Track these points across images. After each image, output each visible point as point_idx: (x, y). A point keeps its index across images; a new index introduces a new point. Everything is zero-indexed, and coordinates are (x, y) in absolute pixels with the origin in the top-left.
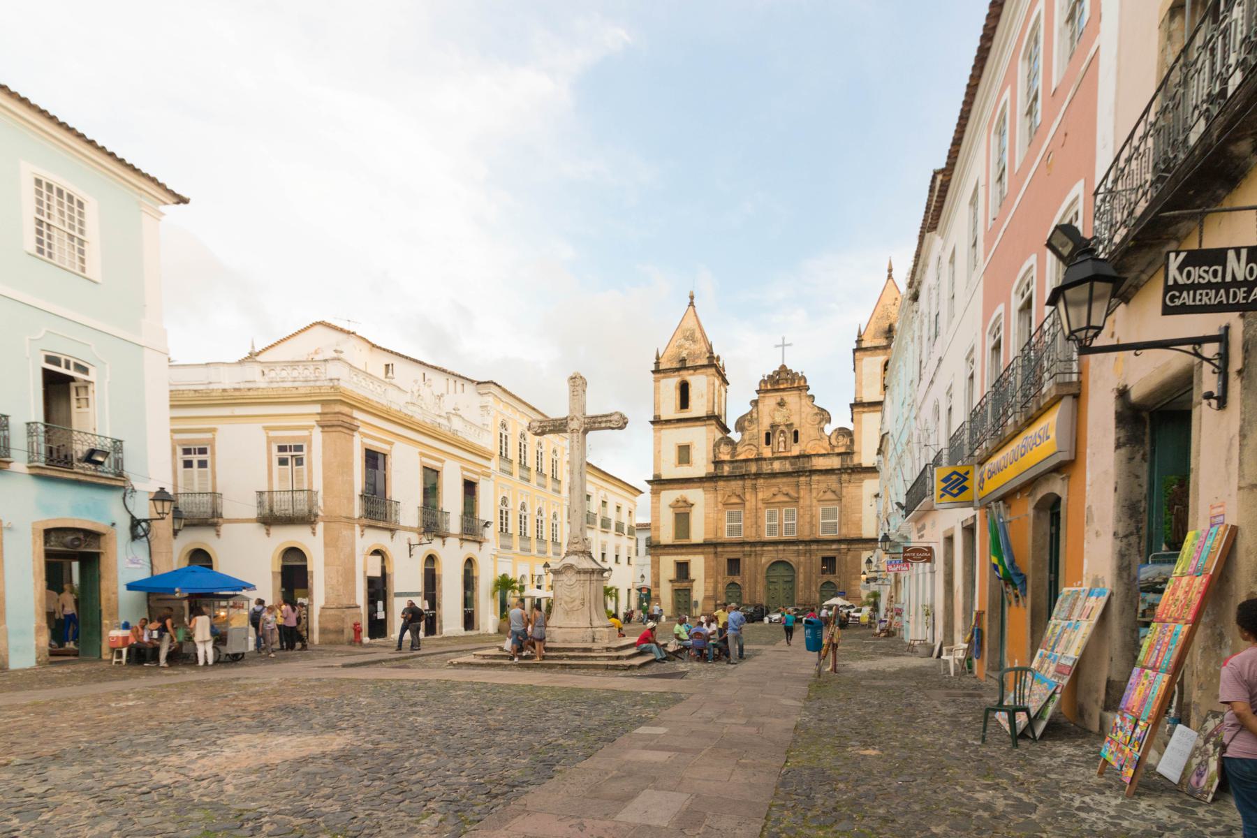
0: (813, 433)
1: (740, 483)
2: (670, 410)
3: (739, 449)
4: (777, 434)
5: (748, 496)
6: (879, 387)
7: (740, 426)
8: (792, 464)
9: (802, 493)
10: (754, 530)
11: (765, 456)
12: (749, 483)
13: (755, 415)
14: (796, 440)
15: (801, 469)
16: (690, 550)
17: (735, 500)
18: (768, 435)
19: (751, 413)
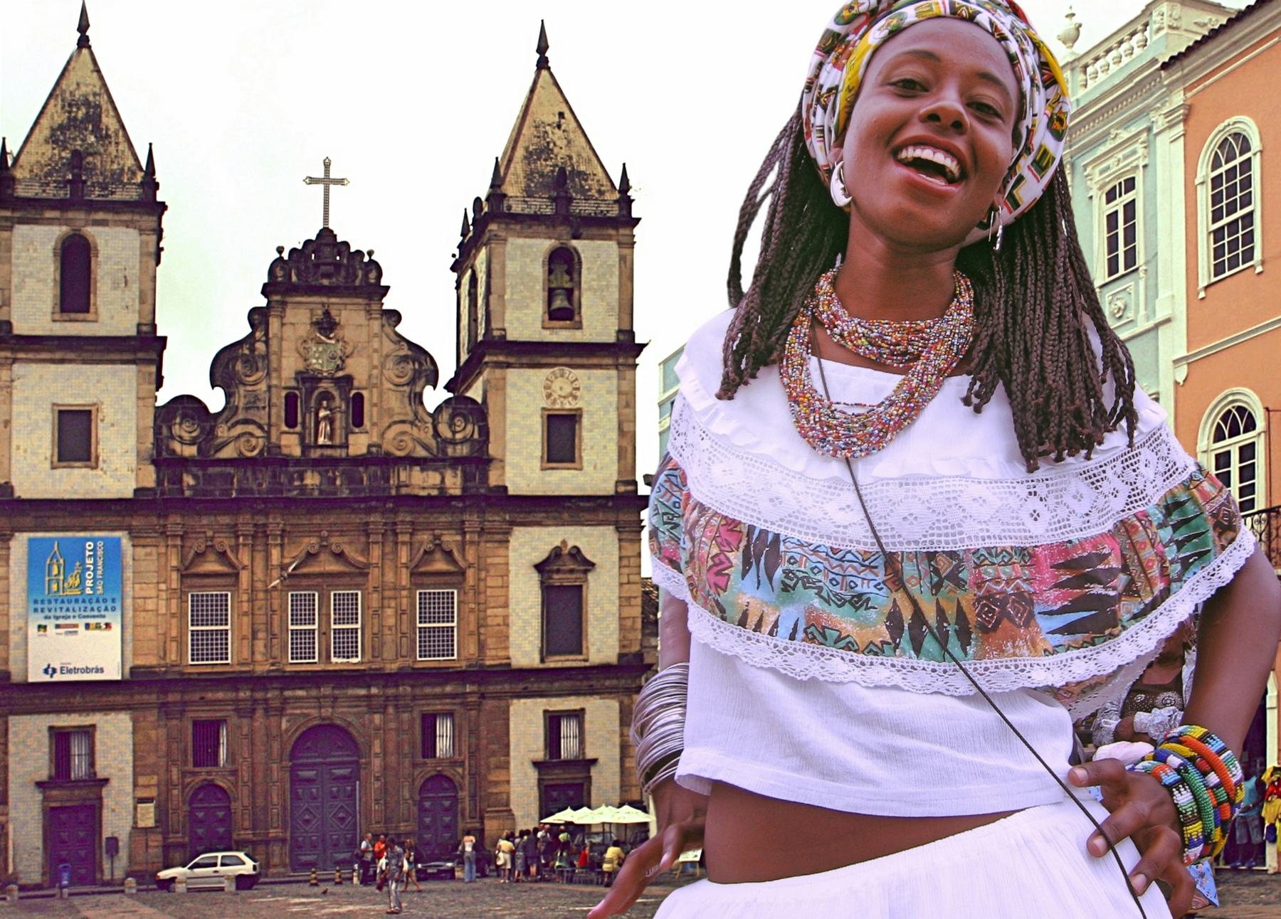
0: (396, 403)
1: (225, 520)
2: (34, 311)
3: (222, 432)
4: (313, 403)
5: (245, 557)
6: (538, 308)
7: (224, 368)
8: (351, 480)
9: (376, 552)
10: (260, 645)
11: (285, 451)
12: (245, 521)
13: (260, 346)
14: (359, 422)
15: (371, 492)
16: (92, 699)
17: (212, 566)
18: (291, 401)
19: (250, 339)
